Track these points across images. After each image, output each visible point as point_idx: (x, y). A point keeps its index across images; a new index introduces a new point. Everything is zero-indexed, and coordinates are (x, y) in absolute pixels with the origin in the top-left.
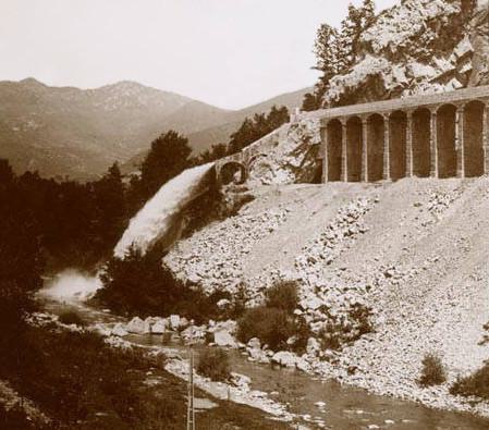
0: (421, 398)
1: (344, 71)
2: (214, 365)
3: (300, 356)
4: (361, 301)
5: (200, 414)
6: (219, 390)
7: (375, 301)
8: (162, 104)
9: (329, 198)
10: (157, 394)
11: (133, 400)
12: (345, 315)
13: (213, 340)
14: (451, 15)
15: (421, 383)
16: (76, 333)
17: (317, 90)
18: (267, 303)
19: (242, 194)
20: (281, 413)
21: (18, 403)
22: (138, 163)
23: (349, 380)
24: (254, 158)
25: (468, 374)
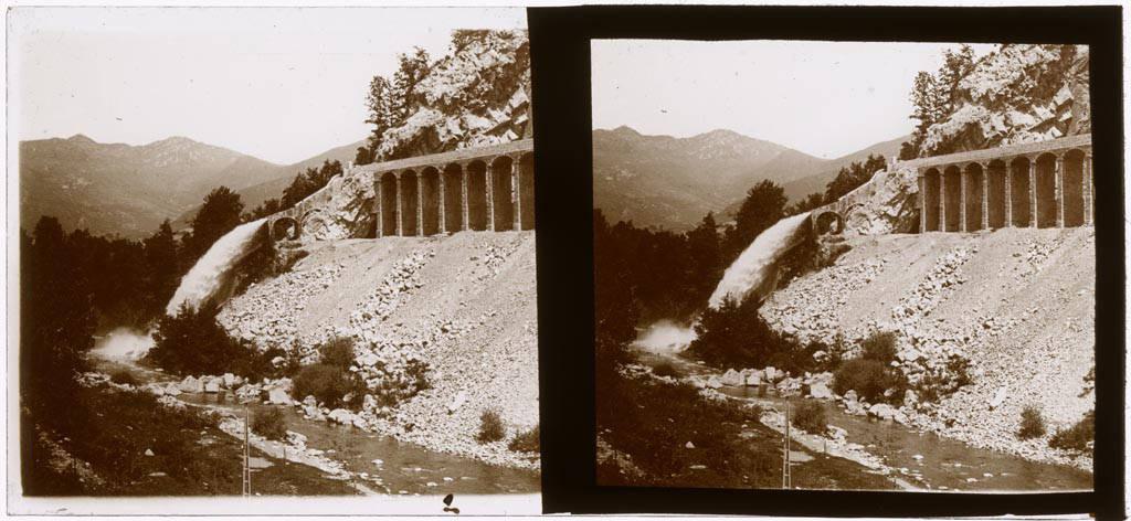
0: (1020, 451)
1: (943, 119)
2: (810, 418)
3: (898, 408)
4: (959, 353)
5: (796, 467)
6: (816, 442)
7: (974, 352)
8: (757, 153)
9: (926, 249)
10: (753, 447)
11: (728, 453)
12: (943, 366)
13: (809, 393)
14: (1050, 63)
15: (1020, 435)
16: (670, 385)
17: (914, 138)
18: (864, 354)
19: (838, 244)
20: (878, 466)
21: (611, 456)
22: (733, 212)
23: (947, 433)
24: (851, 208)
25: (1068, 427)
